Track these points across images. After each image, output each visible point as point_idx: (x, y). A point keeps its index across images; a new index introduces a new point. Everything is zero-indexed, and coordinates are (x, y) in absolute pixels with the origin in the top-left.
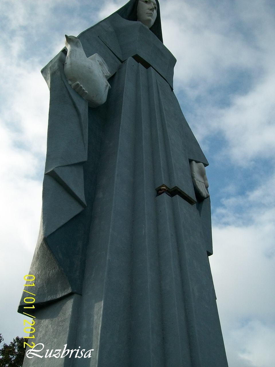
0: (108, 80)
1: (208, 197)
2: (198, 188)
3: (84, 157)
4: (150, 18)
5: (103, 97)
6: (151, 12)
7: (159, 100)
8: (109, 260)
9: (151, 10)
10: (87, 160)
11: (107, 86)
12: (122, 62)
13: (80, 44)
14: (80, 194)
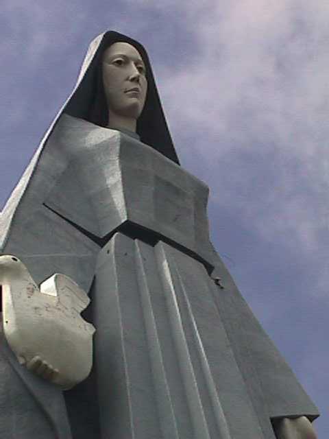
4: (134, 100)
6: (133, 86)
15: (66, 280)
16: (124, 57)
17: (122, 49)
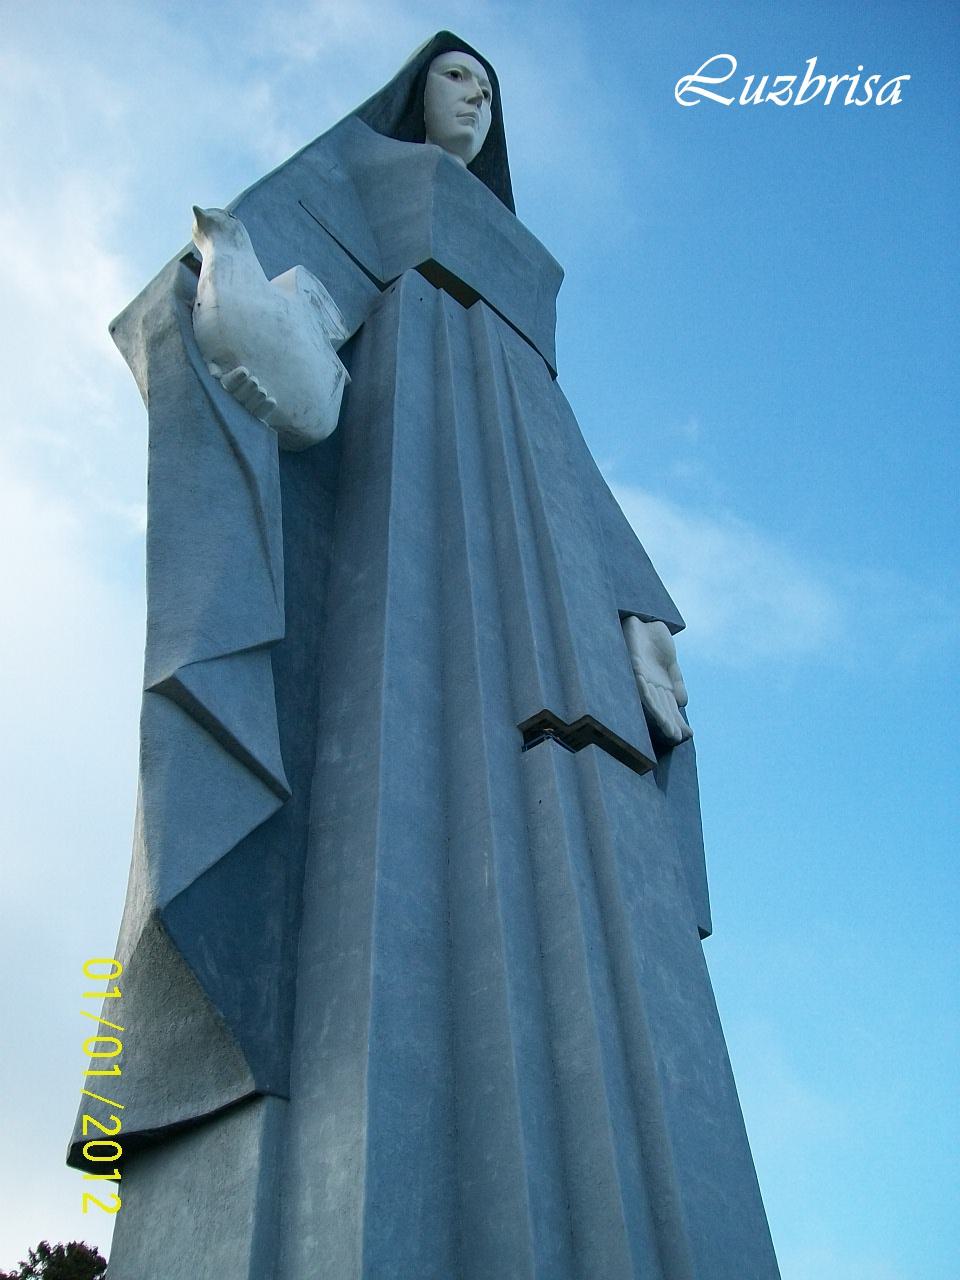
0: (340, 353)
1: (688, 737)
2: (651, 708)
3: (273, 627)
4: (469, 129)
5: (322, 416)
6: (471, 109)
7: (514, 415)
8: (378, 977)
9: (471, 102)
10: (283, 637)
11: (340, 375)
12: (382, 286)
13: (244, 236)
14: (268, 752)
15: (312, 284)
16: (465, 70)
17: (456, 60)
